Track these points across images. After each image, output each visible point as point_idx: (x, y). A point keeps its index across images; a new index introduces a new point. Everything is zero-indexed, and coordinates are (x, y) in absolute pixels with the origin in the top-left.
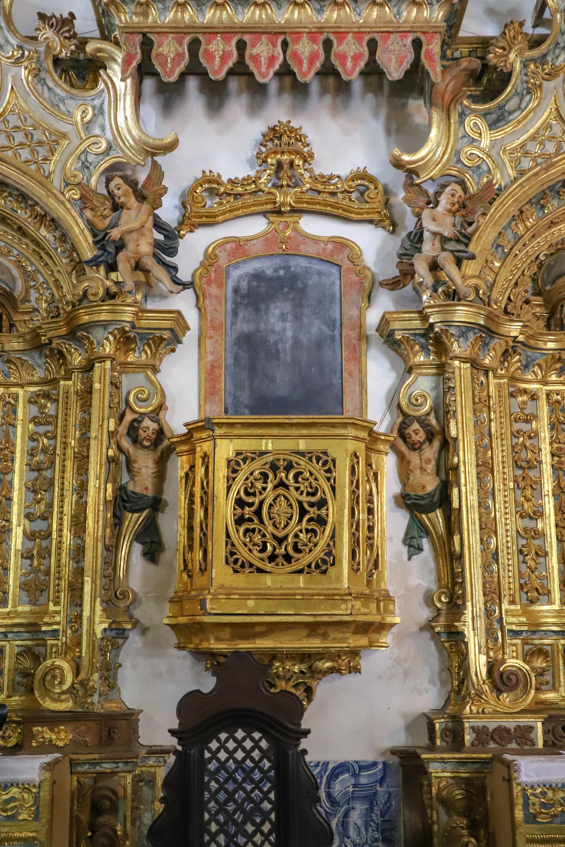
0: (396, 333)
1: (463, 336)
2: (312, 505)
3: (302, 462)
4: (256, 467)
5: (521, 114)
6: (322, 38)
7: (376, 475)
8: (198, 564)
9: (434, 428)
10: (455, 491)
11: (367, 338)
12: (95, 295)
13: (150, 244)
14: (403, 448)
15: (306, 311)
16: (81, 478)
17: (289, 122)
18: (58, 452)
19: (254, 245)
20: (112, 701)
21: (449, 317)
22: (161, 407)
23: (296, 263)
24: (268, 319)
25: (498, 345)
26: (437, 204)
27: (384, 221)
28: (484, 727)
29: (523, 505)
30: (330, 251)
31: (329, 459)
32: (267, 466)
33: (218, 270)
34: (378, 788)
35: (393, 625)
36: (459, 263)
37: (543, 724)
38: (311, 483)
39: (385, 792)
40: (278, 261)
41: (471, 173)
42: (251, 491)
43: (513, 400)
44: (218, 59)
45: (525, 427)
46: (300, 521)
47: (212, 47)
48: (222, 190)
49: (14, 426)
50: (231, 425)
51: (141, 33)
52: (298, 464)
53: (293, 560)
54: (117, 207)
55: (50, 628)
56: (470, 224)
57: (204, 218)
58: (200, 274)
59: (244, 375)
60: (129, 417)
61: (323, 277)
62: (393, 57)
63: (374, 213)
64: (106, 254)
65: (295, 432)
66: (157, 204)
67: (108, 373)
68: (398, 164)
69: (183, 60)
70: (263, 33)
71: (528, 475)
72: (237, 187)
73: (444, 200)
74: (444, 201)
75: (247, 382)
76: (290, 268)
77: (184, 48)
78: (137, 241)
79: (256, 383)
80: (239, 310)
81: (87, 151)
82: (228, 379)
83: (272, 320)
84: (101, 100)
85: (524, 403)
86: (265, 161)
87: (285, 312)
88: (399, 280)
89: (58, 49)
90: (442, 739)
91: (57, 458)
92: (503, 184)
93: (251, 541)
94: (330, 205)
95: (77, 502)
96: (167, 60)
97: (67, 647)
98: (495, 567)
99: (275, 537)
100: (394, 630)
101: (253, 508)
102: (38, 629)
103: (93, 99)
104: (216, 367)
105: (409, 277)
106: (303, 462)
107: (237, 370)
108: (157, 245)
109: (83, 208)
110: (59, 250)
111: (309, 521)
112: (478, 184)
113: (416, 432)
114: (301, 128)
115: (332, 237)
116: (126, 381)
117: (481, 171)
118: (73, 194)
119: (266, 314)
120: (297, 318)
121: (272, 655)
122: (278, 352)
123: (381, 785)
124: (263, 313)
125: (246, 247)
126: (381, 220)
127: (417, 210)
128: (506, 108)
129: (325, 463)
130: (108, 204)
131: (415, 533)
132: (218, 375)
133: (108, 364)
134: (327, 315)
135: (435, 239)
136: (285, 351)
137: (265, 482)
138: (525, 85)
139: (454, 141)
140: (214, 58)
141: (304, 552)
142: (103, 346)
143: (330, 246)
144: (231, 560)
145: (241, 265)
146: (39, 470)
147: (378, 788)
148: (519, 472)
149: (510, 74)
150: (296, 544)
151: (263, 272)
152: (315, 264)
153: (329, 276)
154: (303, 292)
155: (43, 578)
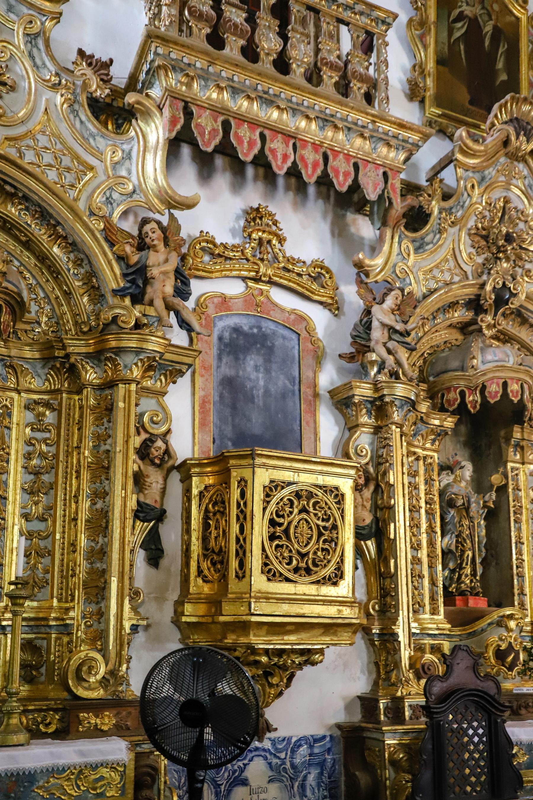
0: (356, 397)
3: (319, 494)
8: (234, 571)
9: (371, 475)
15: (274, 366)
16: (93, 486)
18: (61, 459)
22: (169, 431)
23: (266, 325)
24: (245, 367)
33: (208, 318)
34: (327, 756)
38: (325, 511)
39: (331, 759)
40: (253, 321)
46: (318, 541)
49: (9, 428)
52: (316, 495)
59: (227, 411)
61: (286, 342)
64: (134, 287)
75: (230, 419)
76: (261, 328)
79: (237, 421)
83: (249, 369)
84: (130, 146)
86: (250, 236)
91: (61, 465)
99: (299, 553)
103: (122, 143)
115: (295, 310)
119: (244, 364)
120: (268, 371)
123: (328, 754)
124: (241, 362)
125: (230, 304)
133: (133, 387)
136: (258, 396)
141: (320, 567)
142: (131, 370)
143: (293, 317)
145: (224, 318)
147: (327, 756)
151: (241, 327)
154: (271, 350)
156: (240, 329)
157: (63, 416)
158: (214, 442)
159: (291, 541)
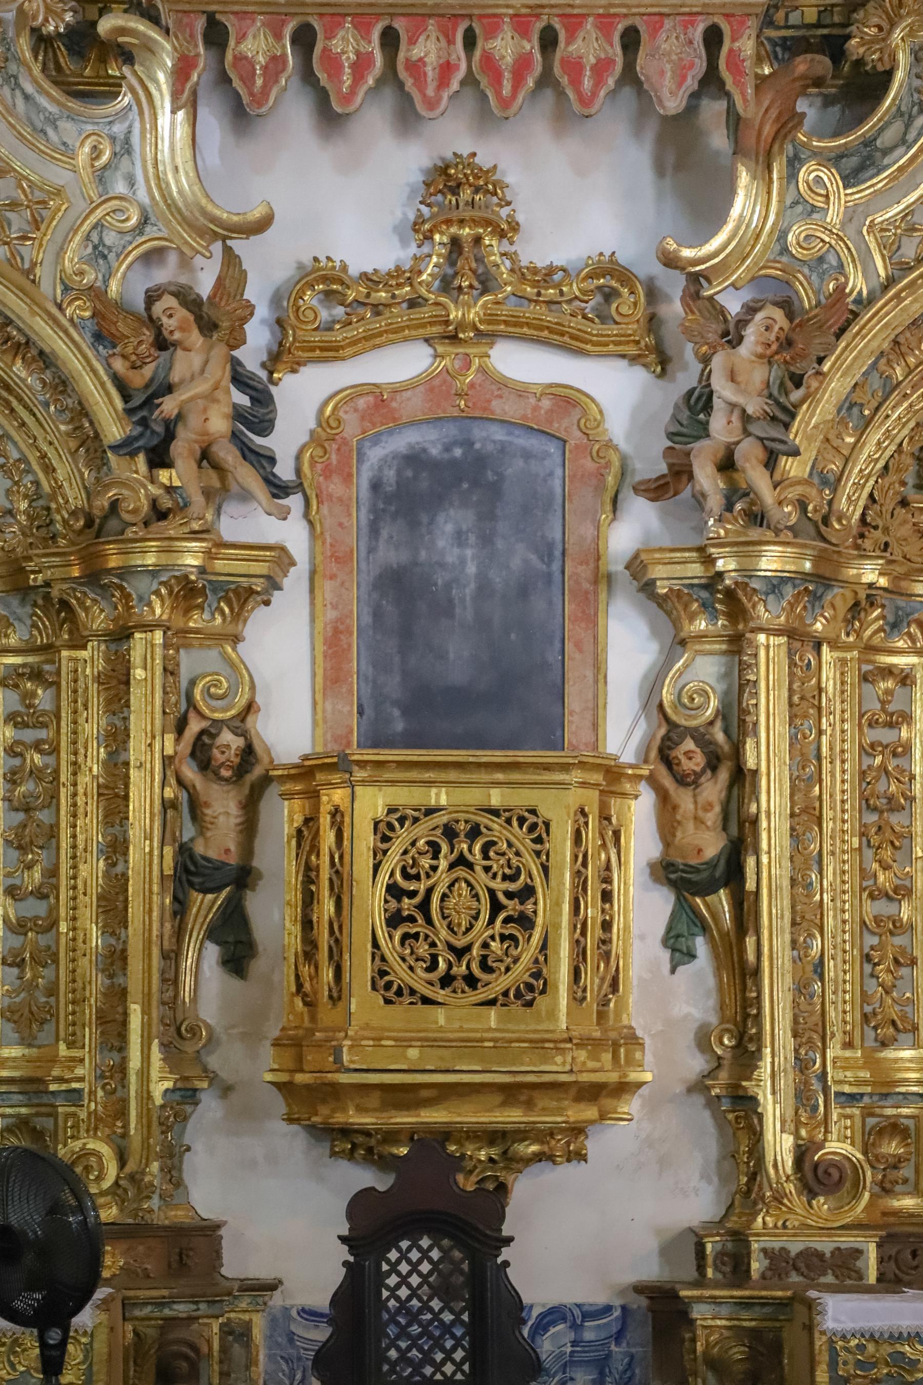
1: (773, 592)
2: (509, 895)
4: (422, 832)
5: (906, 153)
6: (539, 25)
7: (617, 834)
8: (326, 988)
10: (751, 862)
11: (609, 577)
12: (135, 511)
13: (226, 416)
14: (667, 782)
15: (502, 527)
16: (110, 830)
17: (474, 155)
18: (63, 779)
19: (409, 399)
20: (176, 1207)
21: (747, 563)
22: (250, 708)
23: (484, 434)
25: (838, 598)
26: (740, 339)
27: (646, 356)
28: (782, 1249)
29: (875, 876)
30: (546, 413)
31: (540, 821)
32: (439, 832)
34: (613, 1347)
35: (640, 1085)
36: (770, 462)
37: (879, 1246)
39: (626, 1354)
40: (452, 431)
41: (806, 271)
42: (413, 871)
43: (867, 687)
44: (347, 70)
45: (885, 735)
47: (337, 45)
48: (351, 295)
50: (379, 764)
51: (204, 12)
53: (479, 985)
54: (162, 344)
55: (64, 1087)
56: (798, 385)
57: (318, 352)
58: (311, 456)
60: (195, 726)
62: (668, 66)
63: (628, 342)
65: (484, 777)
66: (237, 339)
67: (159, 651)
68: (670, 261)
69: (283, 70)
70: (430, 16)
71: (888, 823)
72: (378, 291)
73: (751, 334)
74: (752, 338)
75: (397, 659)
76: (473, 444)
77: (284, 47)
78: (205, 410)
80: (382, 524)
81: (103, 226)
82: (362, 649)
83: (441, 544)
85: (888, 692)
87: (464, 528)
88: (667, 483)
89: (41, 18)
90: (716, 1268)
91: (63, 790)
92: (865, 292)
93: (412, 953)
94: (548, 328)
95: (106, 874)
96: (255, 70)
97: (99, 1119)
98: (817, 987)
100: (644, 1090)
101: (417, 900)
102: (41, 1088)
104: (341, 632)
105: (685, 478)
106: (496, 825)
107: (379, 637)
108: (238, 414)
109: (110, 356)
110: (52, 408)
111: (507, 921)
112: (817, 293)
113: (689, 755)
114: (495, 167)
115: (551, 386)
116: (188, 663)
117: (825, 266)
118: (79, 307)
120: (486, 540)
121: (445, 1132)
122: (450, 601)
123: (618, 1343)
124: (424, 530)
125: (394, 404)
126: (639, 356)
127: (705, 348)
128: (878, 142)
129: (533, 828)
130: (148, 335)
131: (683, 928)
132: (345, 646)
134: (539, 534)
135: (732, 412)
136: (463, 600)
137: (436, 857)
138: (916, 96)
139: (777, 215)
140: (341, 67)
142: (149, 604)
143: (546, 403)
144: (382, 983)
145: (384, 438)
146: (27, 809)
147: (613, 1347)
148: (871, 818)
149: (889, 75)
150: (484, 958)
151: (424, 450)
152: (518, 436)
153: (544, 459)
155: (44, 999)
156: (423, 456)
157: (64, 695)
158: (361, 712)
159: (433, 926)
